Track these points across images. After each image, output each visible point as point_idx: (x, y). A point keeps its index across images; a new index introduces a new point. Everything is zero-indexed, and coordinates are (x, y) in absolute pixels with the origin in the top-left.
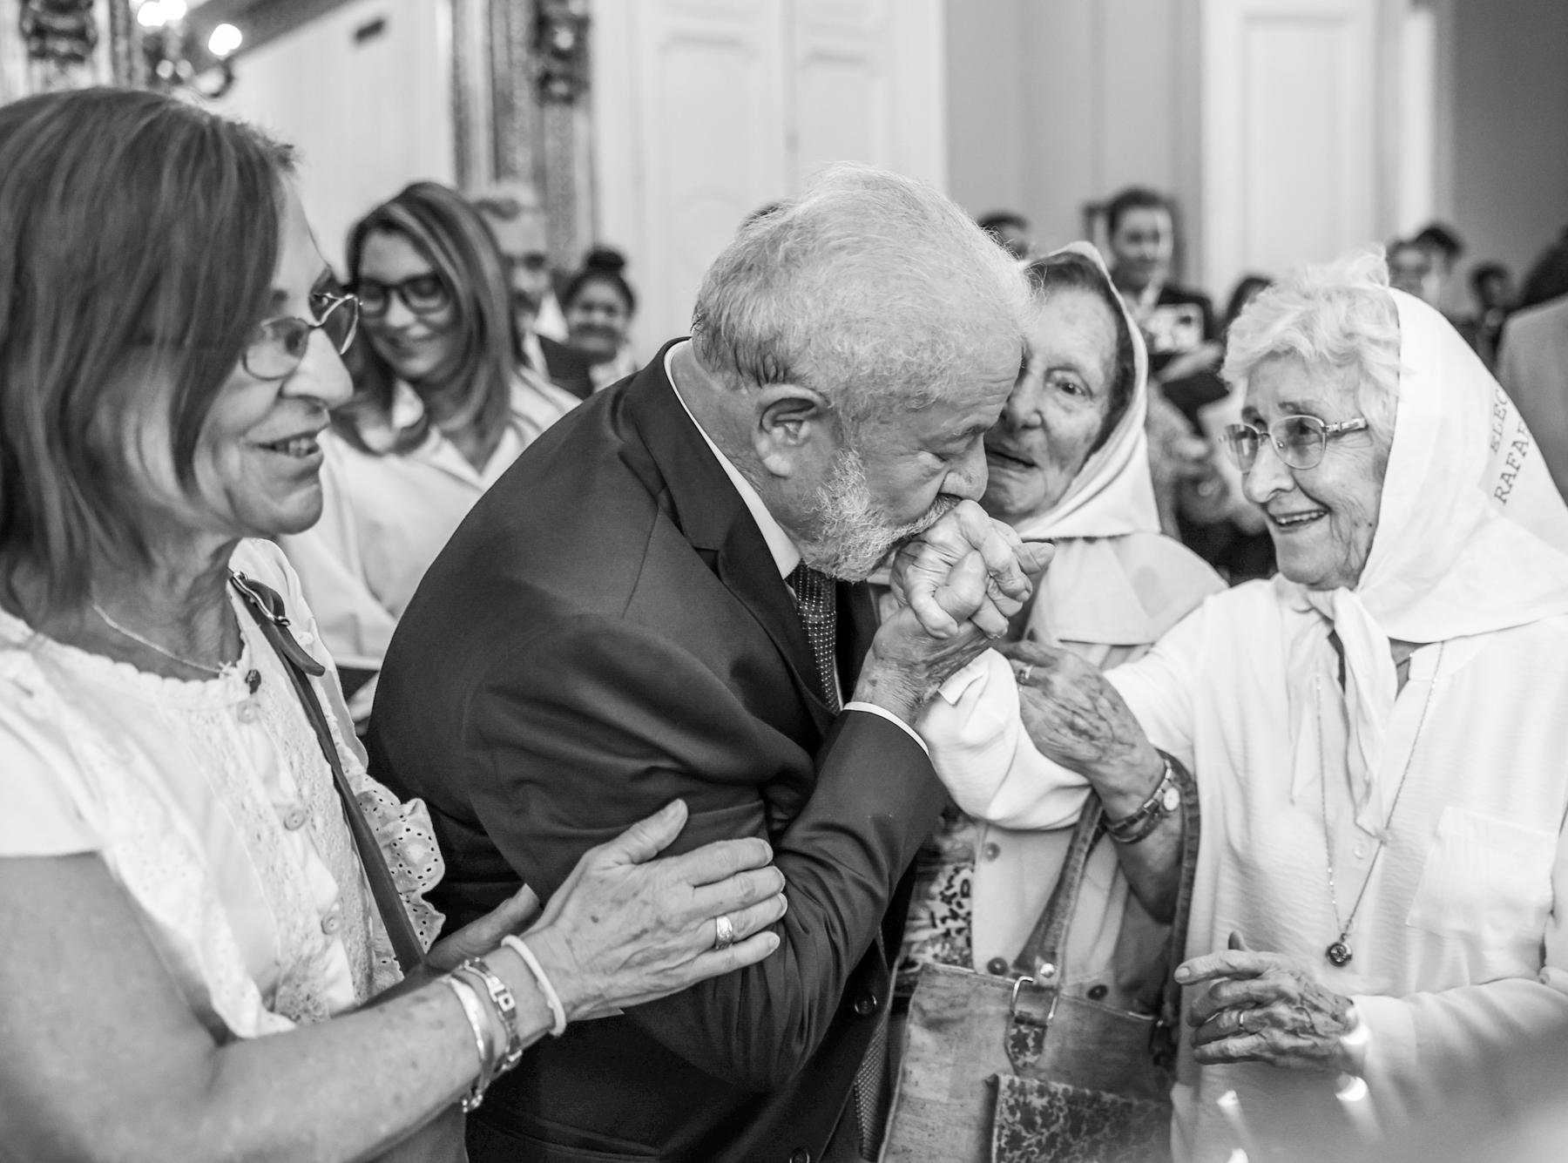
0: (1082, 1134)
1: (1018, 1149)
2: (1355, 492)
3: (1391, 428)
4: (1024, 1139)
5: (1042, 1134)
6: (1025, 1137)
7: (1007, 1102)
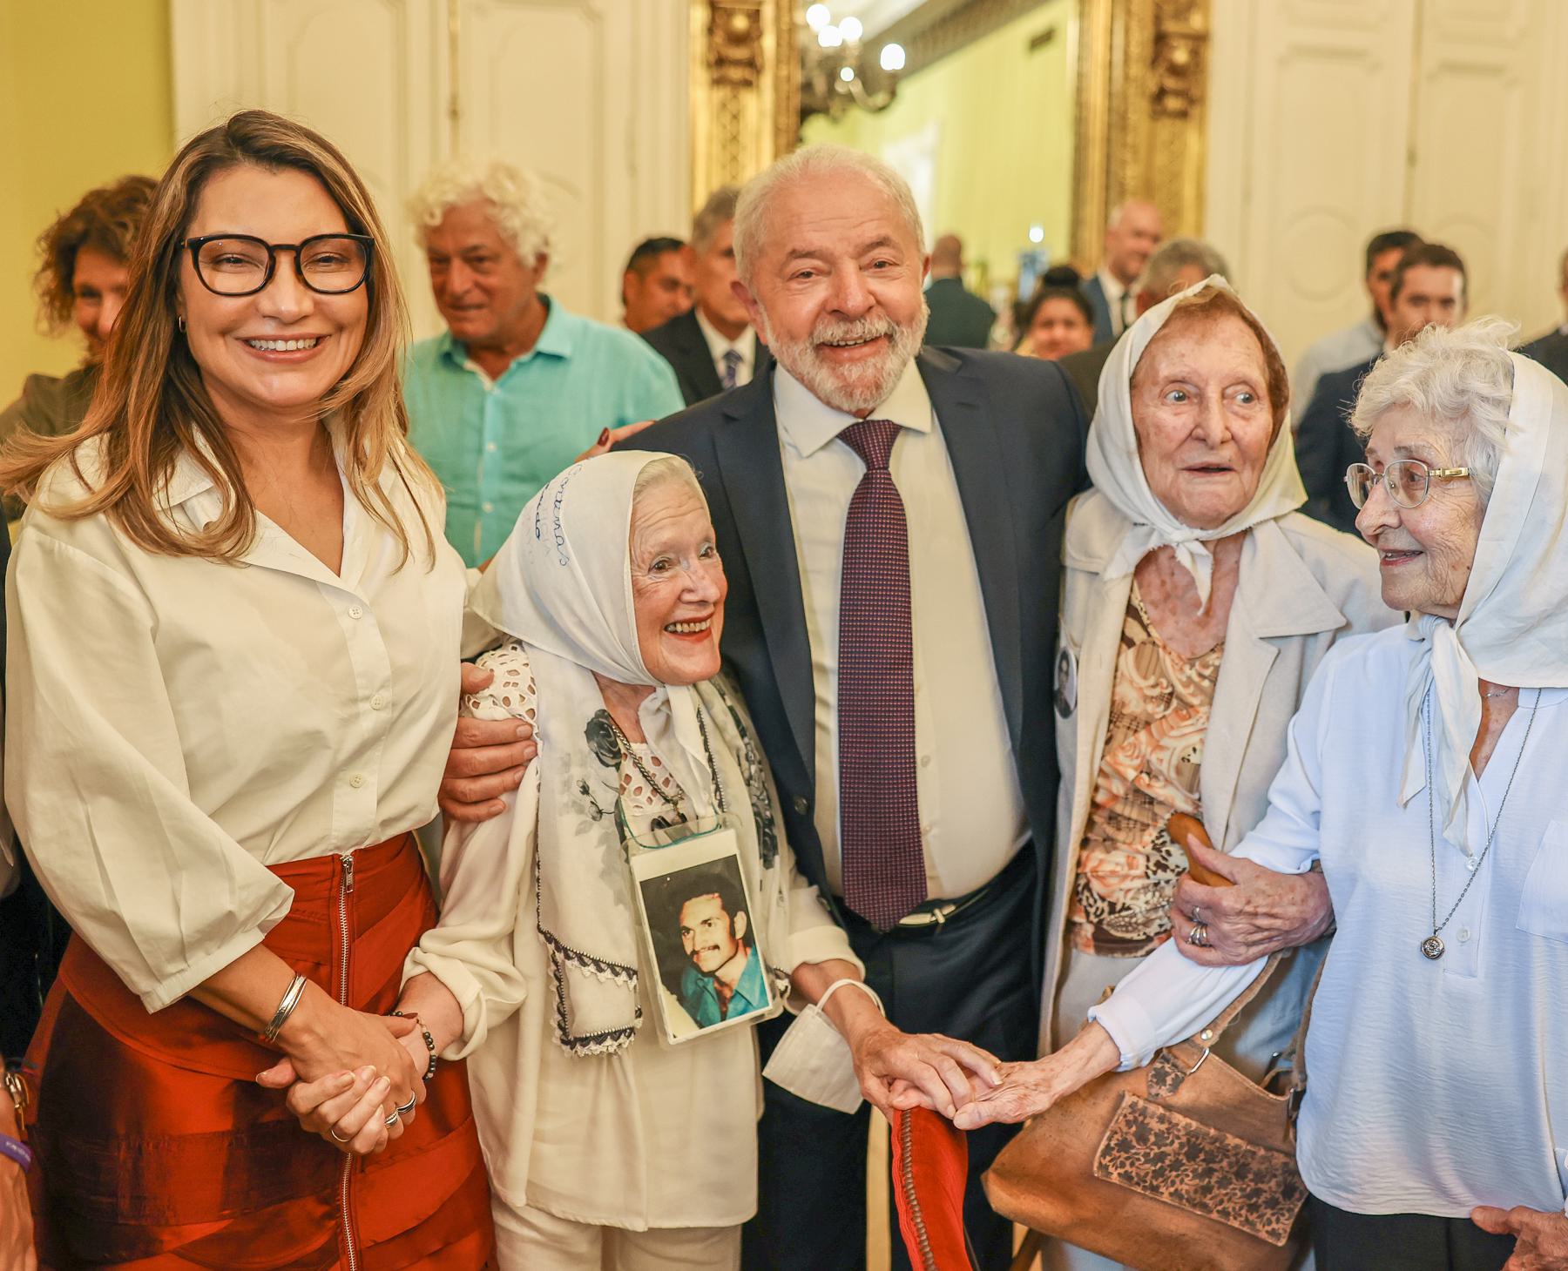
0: (1198, 1160)
1: (1126, 1153)
2: (1453, 538)
3: (1492, 479)
4: (1134, 1147)
5: (1152, 1149)
6: (1134, 1147)
7: (1125, 1116)
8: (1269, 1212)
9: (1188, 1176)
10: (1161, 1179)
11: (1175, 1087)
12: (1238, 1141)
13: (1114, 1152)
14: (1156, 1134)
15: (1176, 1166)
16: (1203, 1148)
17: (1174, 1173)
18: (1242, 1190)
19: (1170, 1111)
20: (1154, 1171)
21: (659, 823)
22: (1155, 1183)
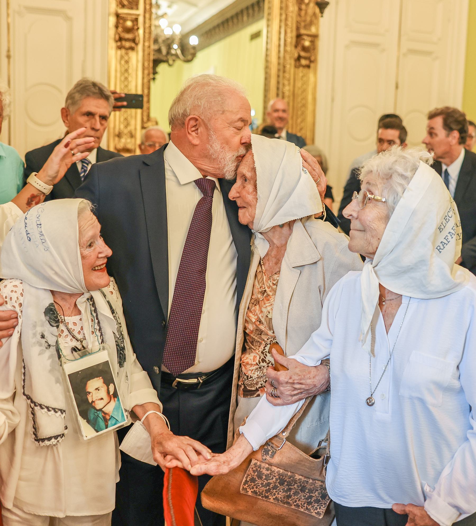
8: (316, 505)
9: (281, 491)
10: (269, 493)
11: (272, 456)
12: (301, 477)
13: (249, 483)
14: (266, 476)
15: (275, 487)
16: (286, 480)
17: (275, 491)
18: (304, 496)
19: (271, 466)
20: (266, 490)
21: (75, 349)
22: (267, 495)
